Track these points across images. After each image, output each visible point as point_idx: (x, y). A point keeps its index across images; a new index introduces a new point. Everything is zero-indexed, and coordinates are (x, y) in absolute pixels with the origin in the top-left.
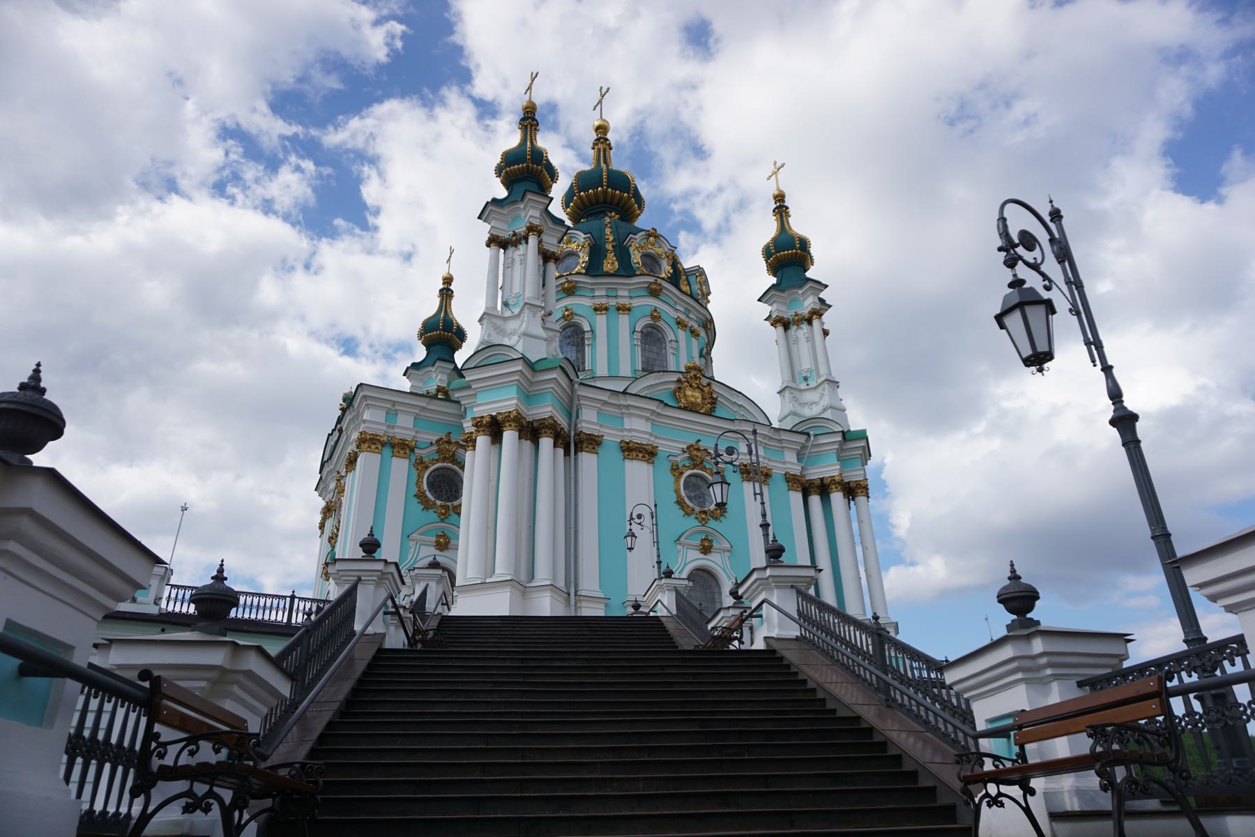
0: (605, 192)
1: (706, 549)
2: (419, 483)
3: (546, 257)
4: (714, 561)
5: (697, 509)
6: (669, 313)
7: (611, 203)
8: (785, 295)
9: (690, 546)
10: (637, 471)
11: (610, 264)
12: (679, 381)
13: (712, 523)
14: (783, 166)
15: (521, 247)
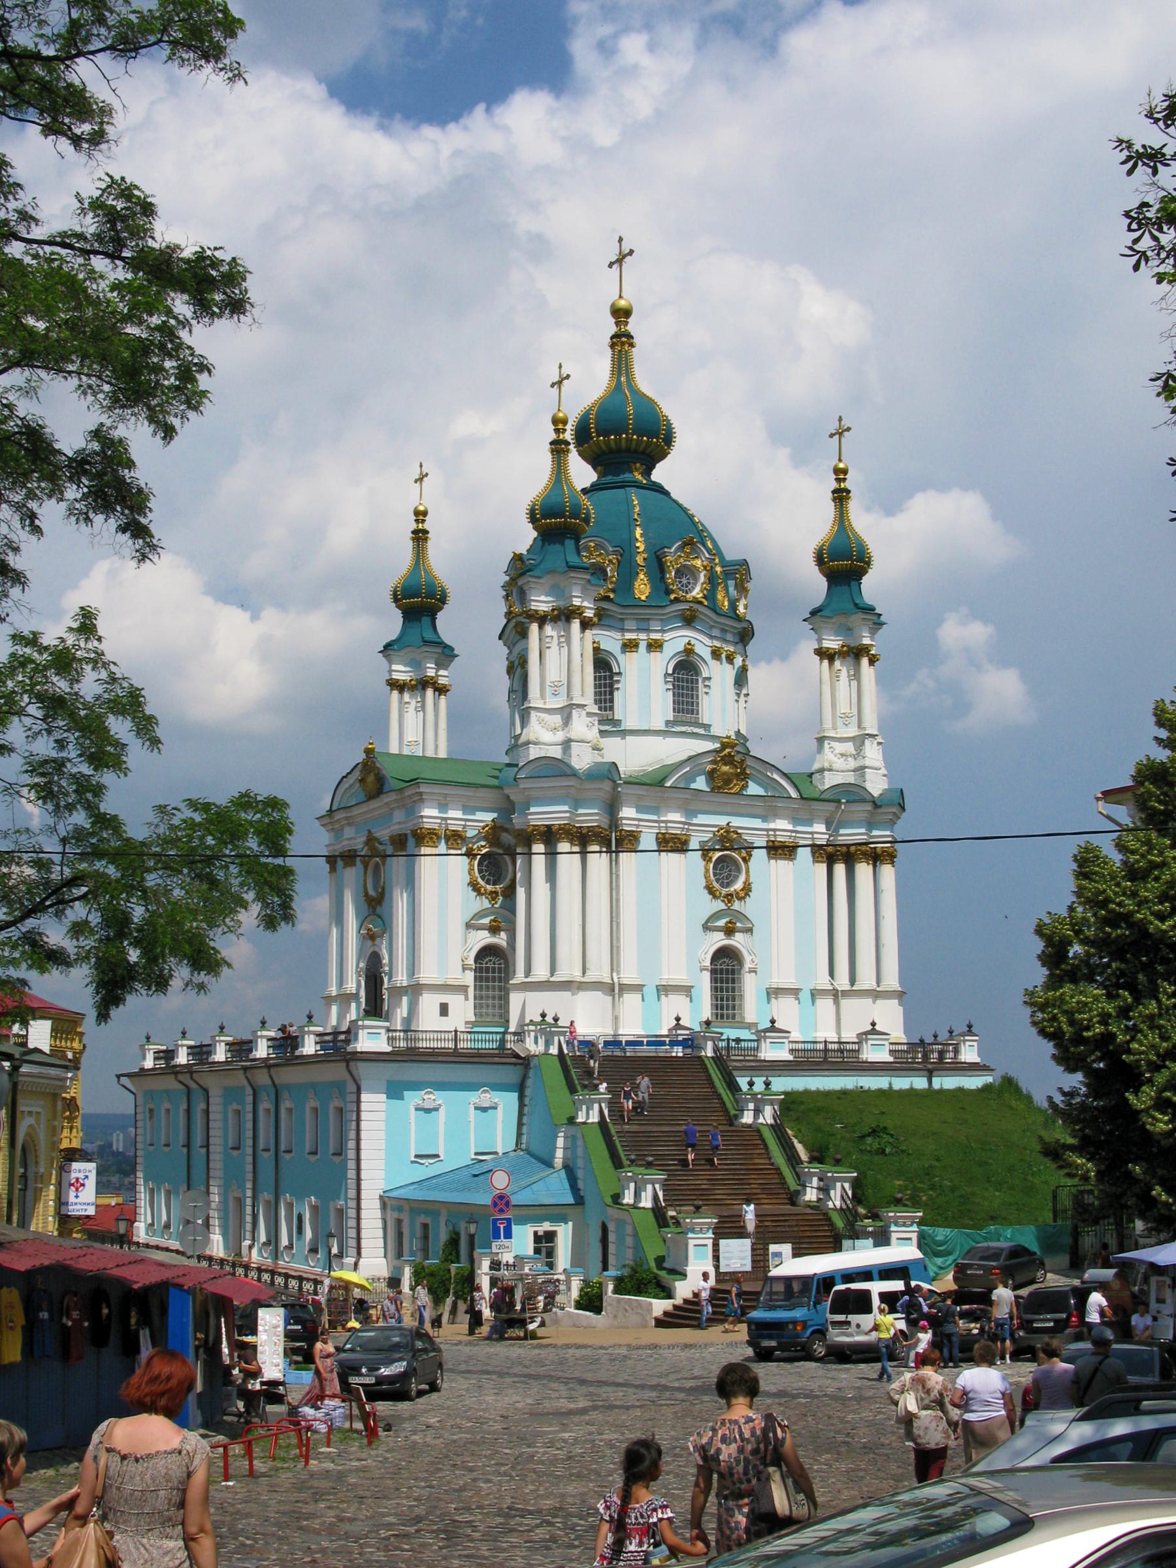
0: (629, 440)
1: (729, 931)
2: (471, 870)
3: (586, 625)
4: (738, 941)
5: (724, 891)
6: (703, 646)
7: (635, 452)
8: (833, 620)
9: (717, 929)
10: (672, 860)
11: (642, 588)
12: (714, 762)
13: (737, 905)
14: (848, 429)
15: (559, 623)
